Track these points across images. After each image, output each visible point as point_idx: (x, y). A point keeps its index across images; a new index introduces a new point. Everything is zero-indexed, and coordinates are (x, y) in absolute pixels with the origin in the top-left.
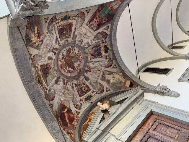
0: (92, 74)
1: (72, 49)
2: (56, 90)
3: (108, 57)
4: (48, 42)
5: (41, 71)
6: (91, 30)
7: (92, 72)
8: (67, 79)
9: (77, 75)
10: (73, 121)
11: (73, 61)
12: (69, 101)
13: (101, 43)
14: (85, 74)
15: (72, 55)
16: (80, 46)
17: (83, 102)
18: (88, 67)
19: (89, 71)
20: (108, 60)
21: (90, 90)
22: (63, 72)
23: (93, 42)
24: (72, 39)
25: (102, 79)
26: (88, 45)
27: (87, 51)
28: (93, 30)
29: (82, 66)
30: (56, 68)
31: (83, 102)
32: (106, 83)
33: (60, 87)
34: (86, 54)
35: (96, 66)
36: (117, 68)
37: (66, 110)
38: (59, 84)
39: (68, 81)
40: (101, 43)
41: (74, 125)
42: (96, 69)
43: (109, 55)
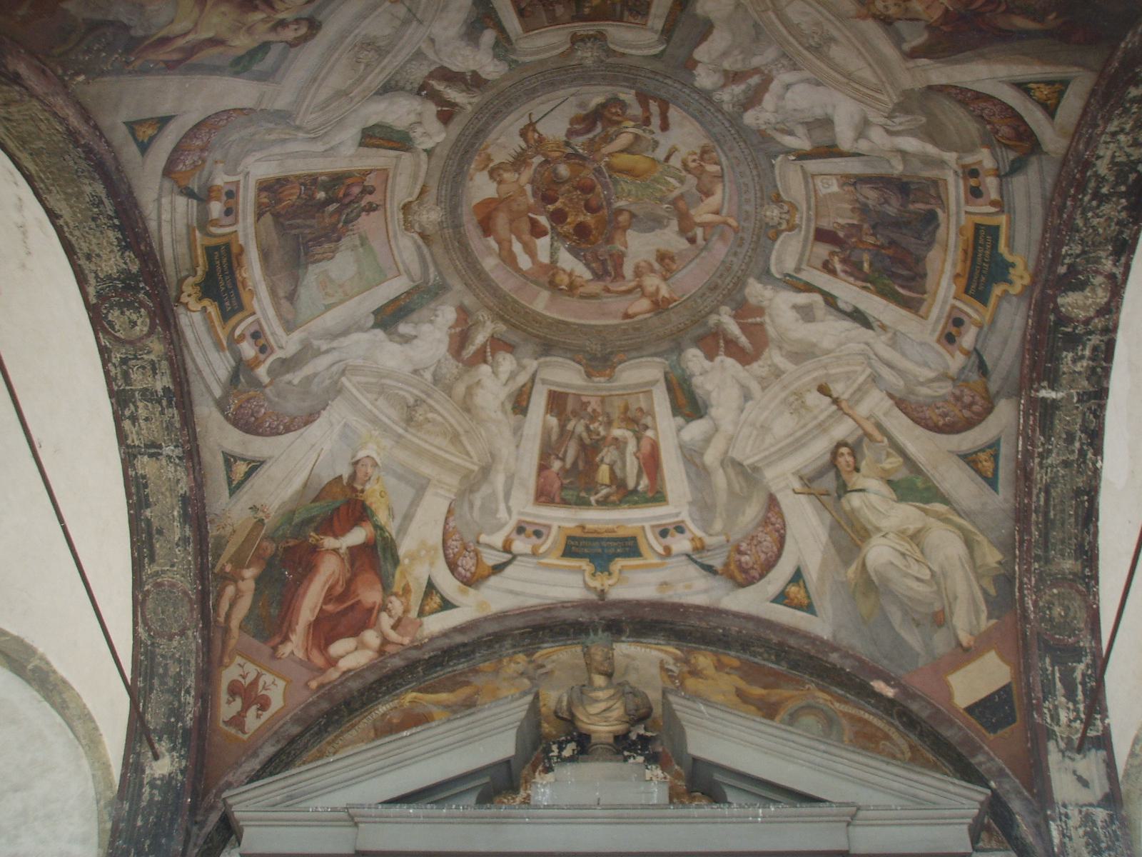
0: (755, 386)
1: (636, 110)
2: (356, 370)
3: (968, 339)
4: (379, 27)
5: (259, 216)
6: (872, 29)
7: (757, 367)
8: (502, 327)
9: (615, 327)
10: (355, 631)
11: (621, 203)
12: (421, 487)
13: (955, 189)
14: (694, 358)
15: (625, 160)
16: (734, 121)
17: (534, 554)
18: (744, 310)
19: (742, 350)
20: (956, 362)
21: (657, 496)
22: (490, 264)
23: (877, 135)
24: (656, 37)
25: (809, 482)
26: (821, 137)
27: (791, 180)
28: (898, 40)
29: (690, 279)
30: (431, 216)
31: (534, 554)
32: (824, 537)
34: (778, 200)
35: (826, 343)
36: (992, 482)
37: (357, 536)
38: (406, 340)
39: (498, 344)
40: (955, 189)
41: (332, 662)
42: (811, 373)
43: (987, 329)
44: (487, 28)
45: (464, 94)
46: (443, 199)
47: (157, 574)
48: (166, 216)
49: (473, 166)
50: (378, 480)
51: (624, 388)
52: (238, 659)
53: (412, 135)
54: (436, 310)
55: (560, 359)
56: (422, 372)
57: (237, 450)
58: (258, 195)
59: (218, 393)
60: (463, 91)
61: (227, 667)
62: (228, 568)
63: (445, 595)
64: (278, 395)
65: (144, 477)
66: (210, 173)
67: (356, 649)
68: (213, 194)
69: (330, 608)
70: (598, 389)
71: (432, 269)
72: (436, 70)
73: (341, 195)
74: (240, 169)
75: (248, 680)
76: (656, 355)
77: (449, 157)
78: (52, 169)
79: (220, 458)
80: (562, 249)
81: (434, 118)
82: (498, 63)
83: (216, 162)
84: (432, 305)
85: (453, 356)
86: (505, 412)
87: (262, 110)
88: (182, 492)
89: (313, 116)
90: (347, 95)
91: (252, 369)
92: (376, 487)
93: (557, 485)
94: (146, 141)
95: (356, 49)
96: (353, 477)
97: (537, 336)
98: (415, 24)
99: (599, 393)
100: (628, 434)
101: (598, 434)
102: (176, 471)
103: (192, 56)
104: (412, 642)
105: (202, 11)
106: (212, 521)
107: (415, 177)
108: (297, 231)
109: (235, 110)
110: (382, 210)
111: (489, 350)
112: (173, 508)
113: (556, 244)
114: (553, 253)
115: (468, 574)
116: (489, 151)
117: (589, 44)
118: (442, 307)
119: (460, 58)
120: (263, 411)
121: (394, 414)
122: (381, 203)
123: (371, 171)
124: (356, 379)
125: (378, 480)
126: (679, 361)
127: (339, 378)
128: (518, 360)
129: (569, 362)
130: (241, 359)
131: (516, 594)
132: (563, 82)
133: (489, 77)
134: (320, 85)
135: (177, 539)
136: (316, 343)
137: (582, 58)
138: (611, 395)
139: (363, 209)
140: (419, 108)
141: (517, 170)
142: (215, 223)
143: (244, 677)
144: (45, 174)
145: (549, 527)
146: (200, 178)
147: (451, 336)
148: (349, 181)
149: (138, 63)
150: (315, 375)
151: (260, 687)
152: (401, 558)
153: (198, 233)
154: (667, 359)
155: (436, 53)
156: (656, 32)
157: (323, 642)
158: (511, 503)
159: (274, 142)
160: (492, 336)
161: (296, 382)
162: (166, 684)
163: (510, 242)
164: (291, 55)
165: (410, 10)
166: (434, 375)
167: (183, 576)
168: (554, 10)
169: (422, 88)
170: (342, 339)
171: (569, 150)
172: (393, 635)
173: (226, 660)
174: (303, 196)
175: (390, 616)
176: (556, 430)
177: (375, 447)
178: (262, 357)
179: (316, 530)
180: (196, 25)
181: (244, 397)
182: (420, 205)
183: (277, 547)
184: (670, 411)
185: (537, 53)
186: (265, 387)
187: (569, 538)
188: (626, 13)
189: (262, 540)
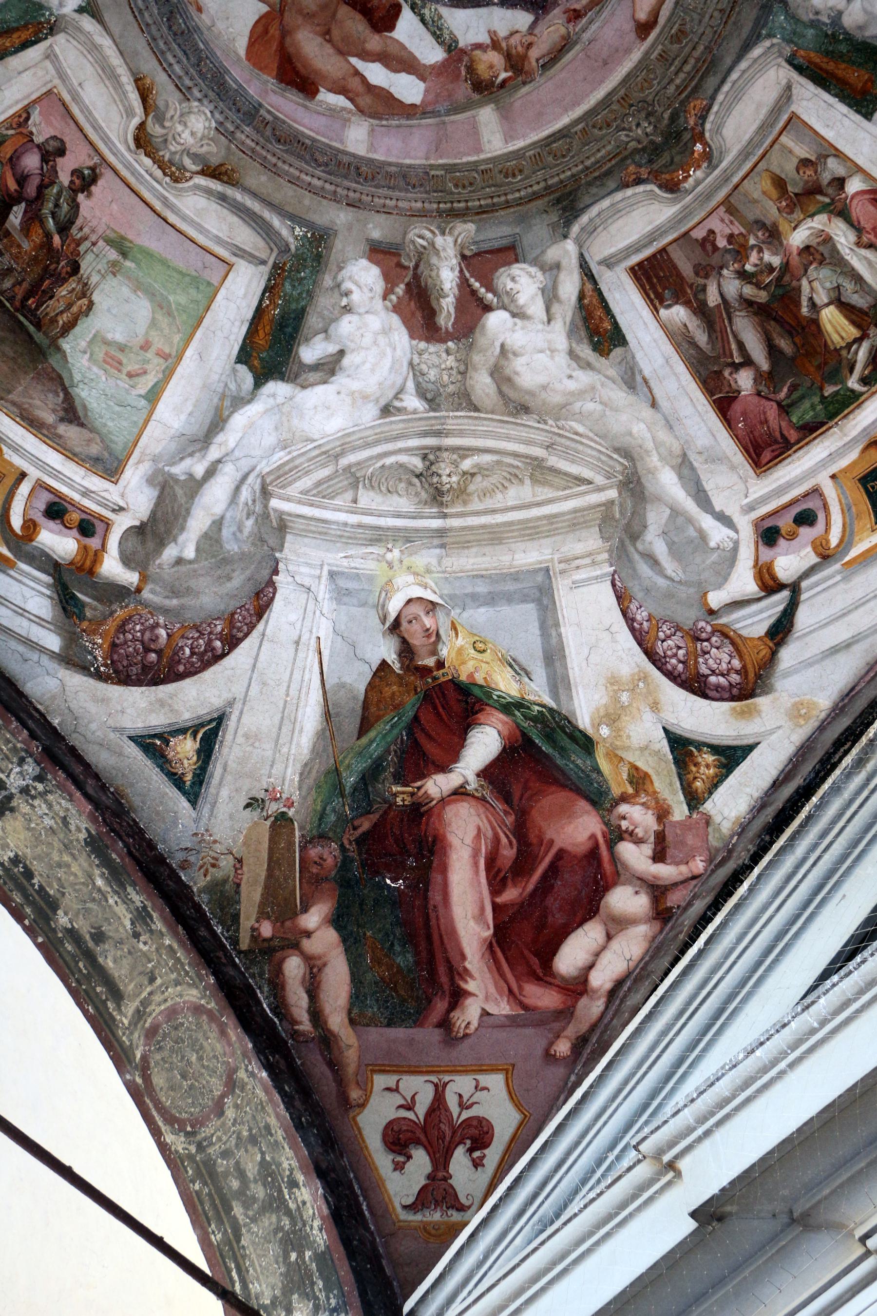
8: (466, 230)
9: (643, 65)
17: (826, 556)
31: (826, 556)
33: (365, 398)
46: (188, 82)
47: (140, 1015)
50: (454, 627)
51: (745, 154)
52: (381, 1081)
54: (339, 286)
55: (606, 203)
56: (397, 404)
57: (158, 720)
59: (53, 642)
61: (363, 1106)
62: (266, 930)
63: (715, 742)
64: (175, 593)
65: (16, 860)
67: (609, 937)
69: (510, 895)
70: (708, 196)
71: (276, 222)
73: (12, 186)
75: (421, 1109)
76: (746, 47)
79: (133, 751)
80: (444, 11)
84: (327, 281)
85: (428, 340)
86: (588, 366)
88: (83, 835)
91: (91, 572)
92: (460, 642)
93: (772, 411)
96: (406, 651)
97: (535, 197)
99: (713, 203)
100: (819, 222)
101: (770, 269)
102: (50, 806)
104: (710, 861)
106: (185, 865)
107: (109, 74)
110: (108, 174)
111: (477, 285)
112: (90, 877)
113: (426, 11)
114: (436, 29)
115: (735, 678)
118: (344, 273)
120: (163, 633)
121: (404, 504)
122: (96, 159)
124: (293, 491)
125: (454, 627)
126: (793, 17)
127: (266, 506)
128: (535, 262)
129: (619, 196)
130: (57, 565)
131: (847, 645)
135: (128, 924)
136: (178, 470)
138: (736, 187)
139: (74, 190)
143: (409, 1107)
145: (816, 491)
147: (396, 309)
150: (218, 524)
151: (454, 1108)
152: (590, 731)
154: (770, 36)
157: (535, 961)
158: (717, 509)
160: (464, 257)
161: (190, 553)
162: (254, 1199)
163: (357, 73)
166: (422, 393)
167: (177, 983)
170: (220, 438)
172: (666, 872)
173: (355, 1094)
175: (638, 841)
176: (694, 325)
177: (411, 579)
178: (94, 543)
179: (400, 778)
181: (110, 626)
182: (160, 119)
183: (342, 848)
184: (858, 118)
186: (139, 590)
187: (864, 480)
189: (303, 849)
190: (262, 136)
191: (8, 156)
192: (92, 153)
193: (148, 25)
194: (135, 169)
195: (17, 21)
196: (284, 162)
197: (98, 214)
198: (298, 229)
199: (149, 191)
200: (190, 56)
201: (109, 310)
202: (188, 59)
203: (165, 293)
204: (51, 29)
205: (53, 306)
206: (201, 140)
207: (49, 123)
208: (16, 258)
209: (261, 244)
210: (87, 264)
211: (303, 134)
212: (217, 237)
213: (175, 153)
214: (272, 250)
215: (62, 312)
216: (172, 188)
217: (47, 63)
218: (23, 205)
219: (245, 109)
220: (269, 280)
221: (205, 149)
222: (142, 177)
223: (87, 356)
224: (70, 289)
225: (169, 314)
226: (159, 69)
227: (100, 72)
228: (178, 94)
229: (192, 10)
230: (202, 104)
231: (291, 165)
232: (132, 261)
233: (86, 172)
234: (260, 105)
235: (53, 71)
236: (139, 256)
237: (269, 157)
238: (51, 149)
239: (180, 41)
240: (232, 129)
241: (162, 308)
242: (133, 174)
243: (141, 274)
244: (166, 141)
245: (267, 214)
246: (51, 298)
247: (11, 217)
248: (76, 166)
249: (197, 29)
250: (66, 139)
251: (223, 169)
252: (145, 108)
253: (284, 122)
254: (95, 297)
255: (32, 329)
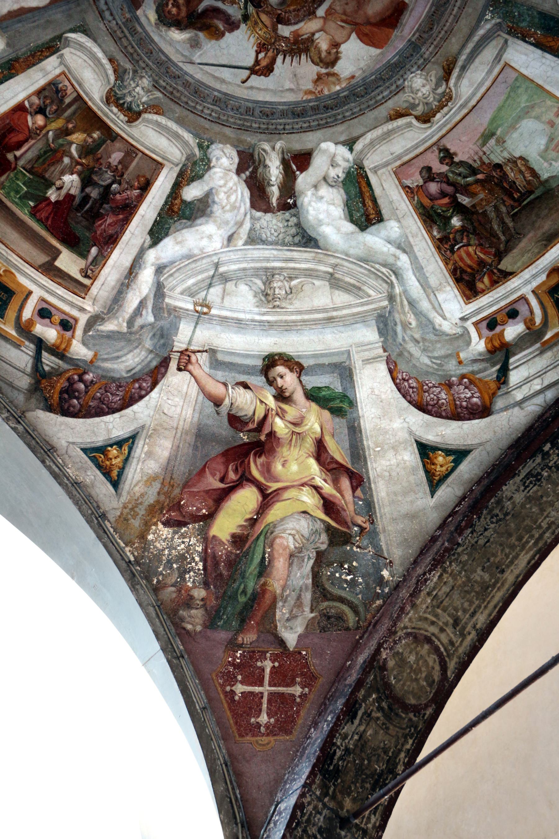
5: (507, 275)
24: (66, 52)
44: (183, 202)
45: (268, 162)
46: (394, 87)
48: (537, 385)
49: (338, 88)
53: (342, 176)
58: (483, 292)
60: (266, 166)
66: (475, 361)
68: (497, 344)
71: (481, 32)
72: (259, 210)
73: (446, 200)
74: (459, 331)
77: (344, 120)
78: (513, 540)
81: (311, 170)
82: (214, 160)
83: (460, 363)
87: (385, 351)
89: (371, 292)
90: (332, 275)
94: (451, 458)
95: (277, 303)
98: (222, 269)
103: (342, 466)
105: (285, 488)
107: (387, 135)
108: (508, 220)
109: (394, 379)
116: (310, 86)
117: (129, 99)
119: (233, 198)
122: (435, 148)
123: (406, 189)
132: (187, 85)
133: (234, 154)
134: (335, 309)
137: (148, 91)
140: (309, 193)
141: (311, 40)
142: (529, 322)
144: (527, 542)
146: (485, 370)
148: (427, 202)
149: (360, 520)
153: (547, 337)
155: (240, 224)
156: (61, 56)
159: (418, 314)
164: (311, 362)
165: (210, 285)
168: (120, 162)
169: (284, 207)
171: (251, 9)
174: (465, 241)
180: (303, 485)
182: (414, 106)
185: (177, 136)
188: (67, 100)
190: (428, 40)
191: (429, 201)
192: (431, 150)
193: (360, 110)
194: (442, 124)
195: (356, 187)
196: (444, 26)
197: (467, 149)
198: (487, 17)
199: (456, 116)
200: (379, 84)
201: (526, 147)
202: (380, 86)
203: (519, 109)
204: (361, 168)
205: (520, 182)
206: (427, 80)
207: (412, 175)
208: (488, 202)
209: (494, 43)
210: (497, 159)
211: (428, 12)
212: (487, 73)
213: (434, 98)
214: (499, 35)
215: (524, 177)
216: (455, 101)
217: (379, 172)
218: (458, 195)
219: (411, 51)
220: (518, 38)
221: (433, 79)
222: (447, 120)
223: (553, 163)
224: (510, 171)
225: (533, 107)
226: (385, 104)
227: (385, 141)
228: (400, 94)
229: (353, 82)
230: (407, 78)
231: (447, 21)
232: (497, 130)
233: (442, 155)
234: (409, 40)
235: (384, 170)
236: (495, 125)
237: (440, 36)
238: (427, 175)
239: (370, 91)
240: (422, 60)
241: (528, 112)
242: (445, 126)
243: (506, 125)
244: (427, 103)
245: (476, 38)
246: (515, 183)
247: (464, 203)
248: (437, 161)
249: (364, 79)
250: (422, 166)
251: (446, 67)
252: (407, 115)
253: (420, 25)
254: (517, 155)
255: (532, 197)
